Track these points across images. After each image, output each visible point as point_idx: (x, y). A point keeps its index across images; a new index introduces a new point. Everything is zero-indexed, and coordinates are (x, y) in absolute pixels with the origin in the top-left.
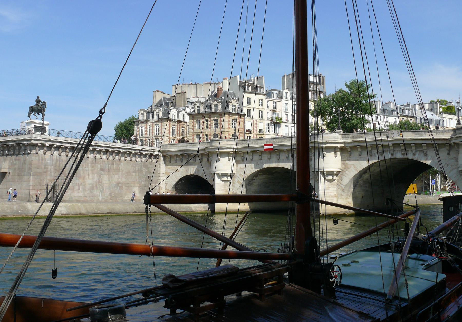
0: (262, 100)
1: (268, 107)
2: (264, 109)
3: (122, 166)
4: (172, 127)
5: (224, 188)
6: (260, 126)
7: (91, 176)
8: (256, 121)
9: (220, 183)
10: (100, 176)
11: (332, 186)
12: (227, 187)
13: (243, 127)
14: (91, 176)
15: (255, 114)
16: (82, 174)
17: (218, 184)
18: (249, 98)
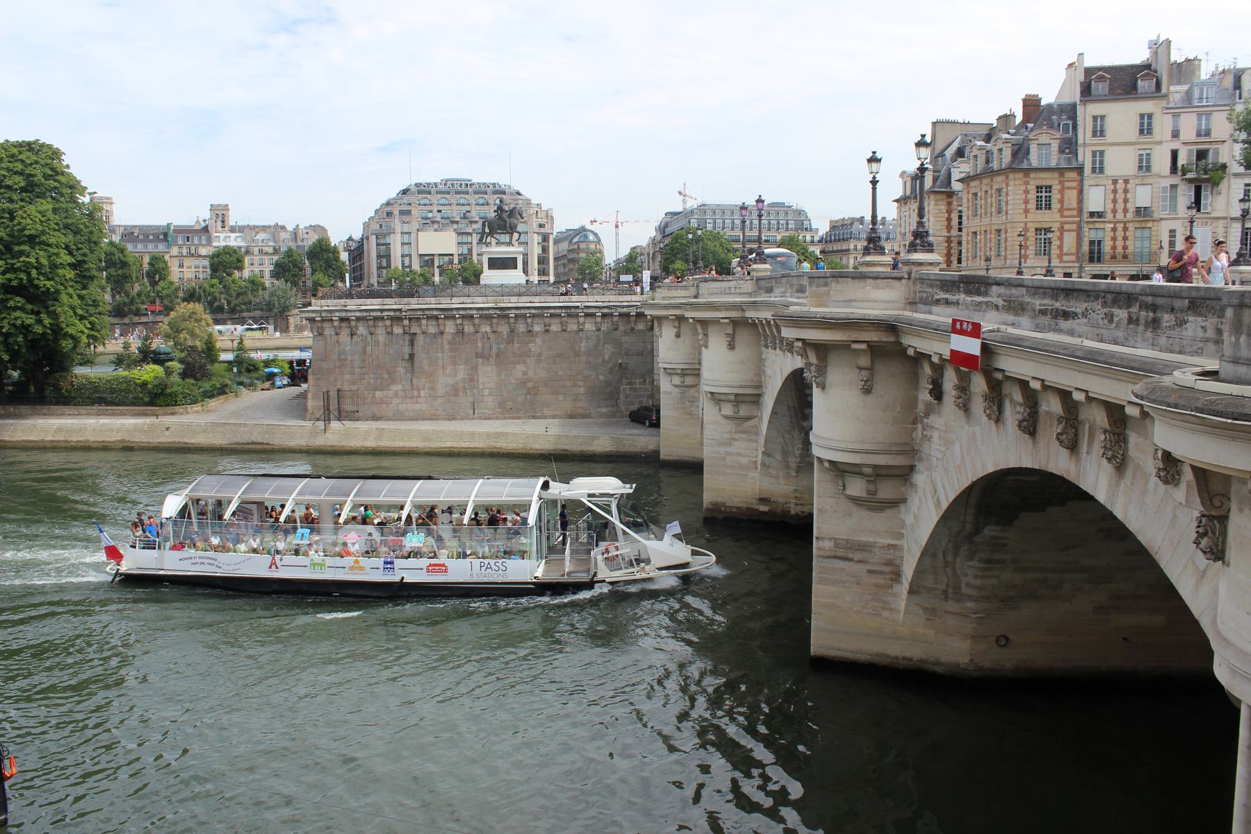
0: (1150, 116)
1: (1176, 134)
2: (1160, 143)
3: (537, 345)
4: (960, 212)
5: (679, 406)
6: (1142, 196)
7: (449, 369)
8: (1126, 181)
9: (671, 393)
10: (475, 368)
11: (744, 436)
12: (687, 403)
13: (1074, 204)
14: (449, 369)
15: (1120, 162)
16: (426, 367)
17: (667, 393)
18: (1103, 117)
